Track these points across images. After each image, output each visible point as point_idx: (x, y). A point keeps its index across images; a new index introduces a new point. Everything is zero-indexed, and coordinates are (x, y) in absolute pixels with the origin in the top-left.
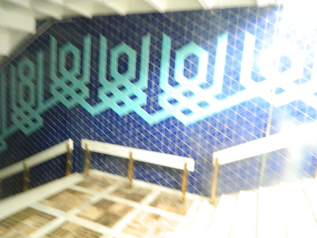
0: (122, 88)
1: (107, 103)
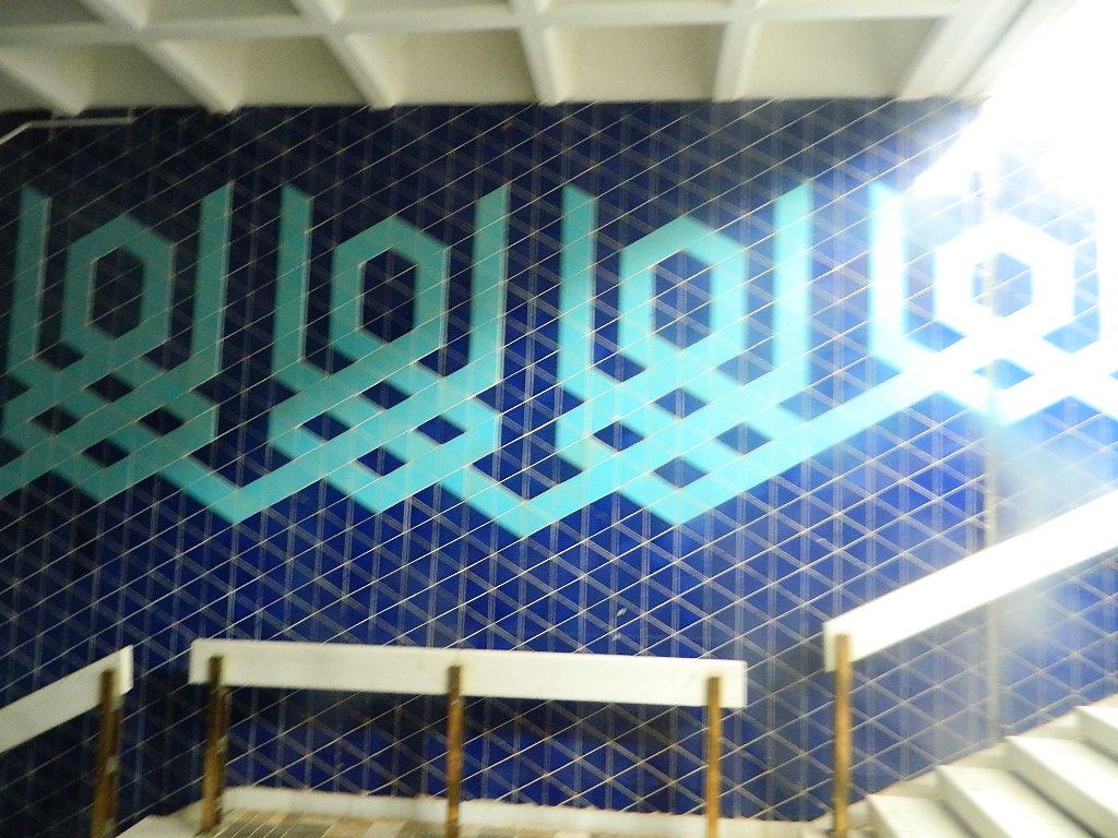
0: (386, 395)
1: (310, 463)
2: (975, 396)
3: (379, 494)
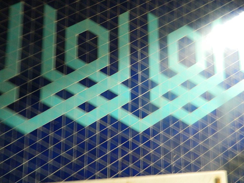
0: (88, 83)
1: (57, 109)
3: (87, 119)
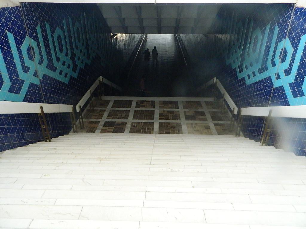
2: (274, 78)
